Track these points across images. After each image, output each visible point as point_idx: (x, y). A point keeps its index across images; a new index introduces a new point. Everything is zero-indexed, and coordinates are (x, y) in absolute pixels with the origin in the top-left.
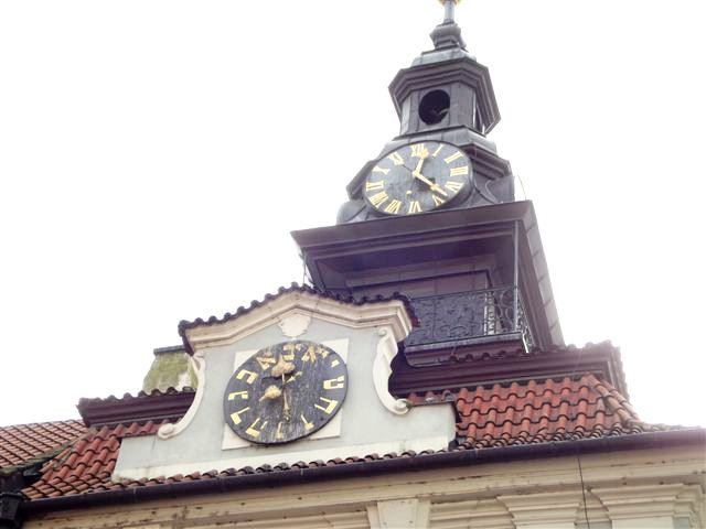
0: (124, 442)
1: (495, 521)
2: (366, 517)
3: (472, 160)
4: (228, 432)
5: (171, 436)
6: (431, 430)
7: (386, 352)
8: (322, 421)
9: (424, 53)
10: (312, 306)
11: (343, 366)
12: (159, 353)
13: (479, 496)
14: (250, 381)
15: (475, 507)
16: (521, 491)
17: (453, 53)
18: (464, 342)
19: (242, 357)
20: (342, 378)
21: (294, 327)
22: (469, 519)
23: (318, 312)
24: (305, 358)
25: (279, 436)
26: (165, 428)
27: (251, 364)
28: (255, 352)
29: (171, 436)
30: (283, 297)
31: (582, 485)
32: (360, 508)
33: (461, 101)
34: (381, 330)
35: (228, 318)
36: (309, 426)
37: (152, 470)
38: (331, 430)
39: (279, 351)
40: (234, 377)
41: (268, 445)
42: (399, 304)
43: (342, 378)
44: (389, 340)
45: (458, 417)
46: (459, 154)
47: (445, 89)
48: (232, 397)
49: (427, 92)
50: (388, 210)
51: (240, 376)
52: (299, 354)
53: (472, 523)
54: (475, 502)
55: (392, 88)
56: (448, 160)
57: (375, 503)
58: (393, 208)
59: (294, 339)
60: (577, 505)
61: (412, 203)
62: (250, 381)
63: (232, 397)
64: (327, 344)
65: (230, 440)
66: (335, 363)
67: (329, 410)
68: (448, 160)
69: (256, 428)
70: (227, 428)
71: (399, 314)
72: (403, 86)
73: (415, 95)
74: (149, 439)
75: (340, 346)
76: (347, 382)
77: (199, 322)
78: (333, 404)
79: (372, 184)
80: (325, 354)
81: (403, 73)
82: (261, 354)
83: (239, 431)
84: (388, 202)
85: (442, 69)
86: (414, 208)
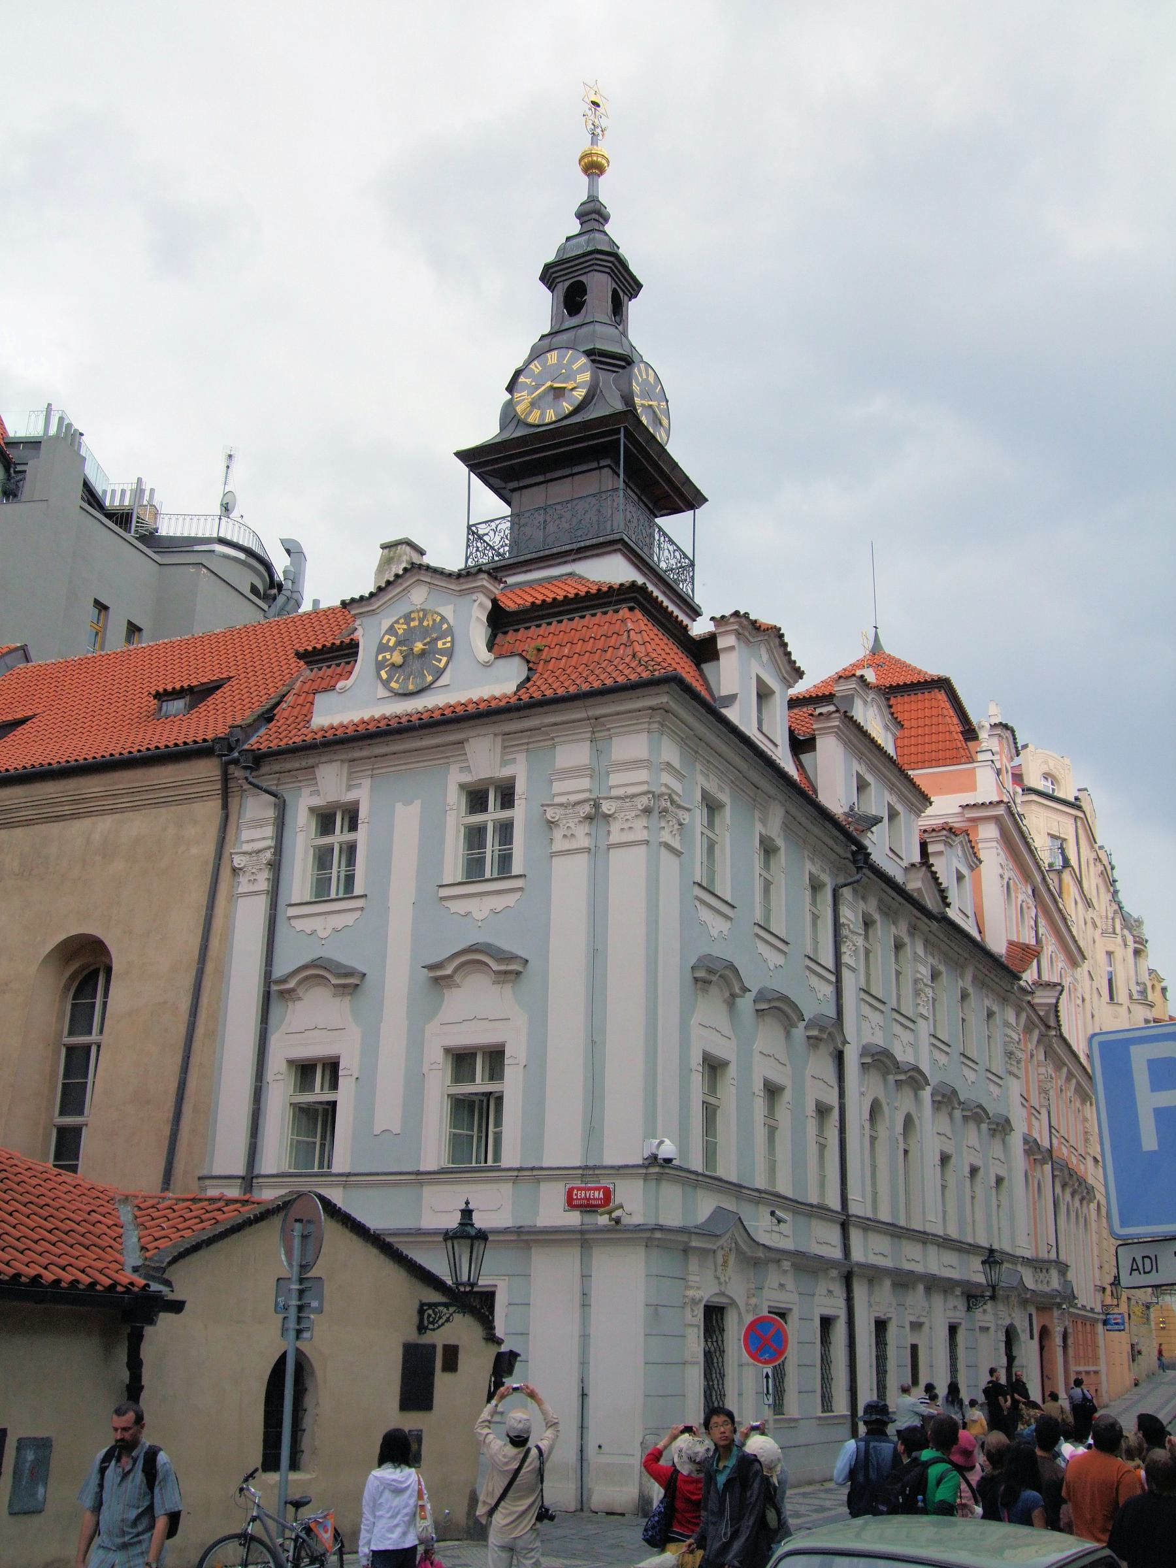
1: (542, 744)
3: (593, 361)
4: (380, 686)
5: (344, 691)
9: (568, 239)
12: (384, 547)
14: (391, 644)
15: (530, 737)
16: (555, 724)
17: (588, 242)
18: (582, 544)
19: (386, 624)
22: (528, 744)
24: (425, 623)
25: (411, 687)
26: (340, 685)
27: (391, 630)
28: (395, 619)
29: (344, 691)
30: (408, 575)
32: (461, 742)
33: (599, 285)
34: (474, 597)
35: (372, 595)
36: (430, 678)
38: (444, 680)
39: (408, 618)
40: (381, 642)
41: (405, 695)
46: (583, 360)
47: (583, 278)
48: (380, 657)
49: (567, 283)
50: (530, 420)
52: (421, 621)
53: (531, 746)
55: (542, 278)
56: (575, 367)
57: (467, 740)
58: (534, 418)
62: (391, 644)
63: (380, 657)
64: (440, 610)
65: (382, 692)
66: (445, 626)
67: (442, 665)
68: (575, 367)
71: (485, 583)
72: (549, 275)
73: (560, 285)
75: (447, 611)
77: (353, 600)
78: (444, 659)
81: (548, 267)
82: (397, 622)
83: (386, 684)
84: (531, 412)
85: (577, 262)
86: (550, 416)
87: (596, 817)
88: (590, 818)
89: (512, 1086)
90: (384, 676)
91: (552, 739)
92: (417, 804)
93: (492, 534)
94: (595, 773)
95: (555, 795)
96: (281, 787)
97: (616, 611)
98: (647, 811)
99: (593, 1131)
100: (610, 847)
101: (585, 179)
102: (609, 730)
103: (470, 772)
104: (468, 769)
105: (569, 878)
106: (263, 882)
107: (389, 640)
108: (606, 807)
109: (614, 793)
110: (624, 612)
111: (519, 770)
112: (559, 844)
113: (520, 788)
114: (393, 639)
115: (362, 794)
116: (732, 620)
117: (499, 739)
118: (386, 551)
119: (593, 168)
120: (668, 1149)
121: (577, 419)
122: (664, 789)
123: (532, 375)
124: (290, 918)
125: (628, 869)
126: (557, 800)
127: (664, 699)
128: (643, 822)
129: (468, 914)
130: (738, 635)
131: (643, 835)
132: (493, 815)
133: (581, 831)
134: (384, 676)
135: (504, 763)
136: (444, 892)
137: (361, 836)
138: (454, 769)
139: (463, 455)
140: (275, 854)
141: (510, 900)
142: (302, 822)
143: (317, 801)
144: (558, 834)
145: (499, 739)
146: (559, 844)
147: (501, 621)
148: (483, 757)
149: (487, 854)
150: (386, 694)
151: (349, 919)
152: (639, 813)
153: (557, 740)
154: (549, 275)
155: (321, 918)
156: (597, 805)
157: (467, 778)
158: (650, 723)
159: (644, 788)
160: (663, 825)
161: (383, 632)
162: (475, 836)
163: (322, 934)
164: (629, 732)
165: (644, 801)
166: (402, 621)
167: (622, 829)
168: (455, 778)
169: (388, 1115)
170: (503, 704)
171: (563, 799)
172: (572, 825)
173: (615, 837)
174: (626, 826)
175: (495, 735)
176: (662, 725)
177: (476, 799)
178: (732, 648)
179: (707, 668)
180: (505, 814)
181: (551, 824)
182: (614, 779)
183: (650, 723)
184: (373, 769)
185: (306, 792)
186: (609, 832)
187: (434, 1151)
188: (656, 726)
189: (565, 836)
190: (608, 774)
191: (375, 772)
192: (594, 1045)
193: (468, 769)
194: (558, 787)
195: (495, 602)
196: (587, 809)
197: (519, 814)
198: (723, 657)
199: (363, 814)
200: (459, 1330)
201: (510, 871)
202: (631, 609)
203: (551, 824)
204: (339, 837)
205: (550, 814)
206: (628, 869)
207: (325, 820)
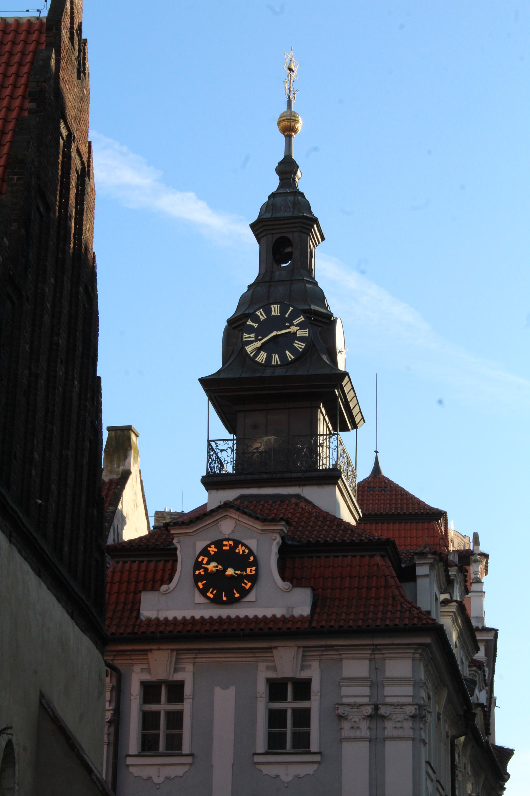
0: (142, 593)
2: (272, 652)
4: (197, 593)
5: (166, 593)
6: (299, 603)
7: (275, 549)
8: (245, 593)
10: (237, 517)
11: (255, 557)
13: (326, 646)
15: (323, 651)
19: (200, 546)
20: (254, 568)
21: (227, 527)
23: (240, 521)
26: (164, 587)
27: (205, 552)
28: (208, 543)
31: (373, 645)
32: (271, 648)
37: (160, 612)
38: (251, 597)
39: (219, 544)
42: (283, 523)
43: (254, 568)
44: (278, 542)
45: (313, 589)
47: (290, 236)
48: (197, 572)
49: (276, 237)
51: (200, 560)
54: (324, 649)
59: (227, 536)
60: (371, 652)
61: (273, 355)
62: (205, 562)
63: (197, 572)
64: (245, 541)
65: (199, 598)
69: (211, 593)
70: (196, 590)
74: (156, 593)
75: (252, 544)
76: (256, 570)
79: (248, 336)
80: (247, 551)
82: (209, 546)
83: (203, 592)
87: (376, 716)
88: (370, 717)
90: (200, 585)
91: (340, 654)
92: (232, 690)
93: (229, 451)
94: (375, 684)
95: (342, 697)
96: (115, 662)
97: (373, 556)
98: (413, 717)
100: (384, 740)
101: (282, 139)
102: (383, 654)
103: (275, 670)
104: (274, 669)
105: (355, 757)
107: (203, 559)
108: (383, 711)
109: (388, 700)
110: (378, 559)
111: (313, 672)
112: (347, 732)
113: (315, 686)
114: (206, 559)
115: (186, 675)
116: (429, 556)
117: (301, 650)
118: (113, 433)
119: (288, 129)
121: (302, 372)
122: (422, 702)
123: (256, 319)
124: (128, 766)
126: (345, 700)
127: (428, 640)
128: (408, 724)
129: (278, 776)
130: (432, 566)
131: (410, 733)
132: (289, 705)
133: (364, 725)
134: (200, 585)
135: (303, 668)
136: (257, 759)
137: (187, 707)
138: (262, 666)
139: (204, 381)
140: (113, 715)
141: (310, 769)
142: (135, 689)
143: (146, 677)
144: (346, 725)
145: (301, 650)
146: (347, 732)
147: (286, 553)
148: (286, 661)
149: (287, 732)
150: (202, 600)
151: (180, 771)
152: (407, 717)
153: (343, 656)
155: (157, 767)
156: (376, 708)
157: (272, 675)
158: (414, 653)
159: (410, 700)
160: (422, 726)
161: (198, 553)
162: (276, 718)
163: (156, 780)
164: (397, 658)
165: (411, 710)
166: (213, 546)
167: (395, 728)
168: (263, 675)
170: (306, 625)
171: (351, 700)
172: (357, 720)
173: (389, 732)
174: (398, 725)
175: (299, 647)
176: (421, 654)
177: (277, 689)
178: (427, 576)
179: (406, 587)
180: (301, 705)
181: (341, 717)
182: (388, 690)
183: (414, 653)
184: (195, 658)
185: (137, 669)
186: (384, 728)
188: (417, 656)
189: (352, 728)
190: (383, 686)
191: (196, 660)
193: (274, 669)
194: (345, 691)
195: (283, 538)
196: (369, 710)
197: (314, 705)
198: (419, 581)
199: (188, 690)
201: (308, 747)
202: (383, 556)
203: (341, 717)
204: (163, 707)
205: (341, 711)
207: (150, 691)
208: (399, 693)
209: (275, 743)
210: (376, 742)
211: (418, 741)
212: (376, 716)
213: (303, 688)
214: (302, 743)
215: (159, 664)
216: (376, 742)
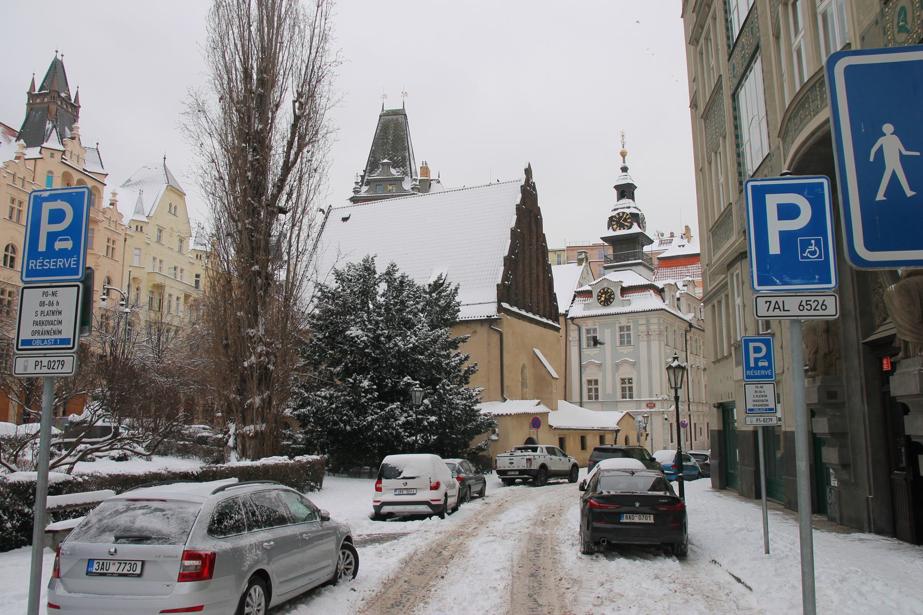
89: (634, 385)
99: (650, 395)
105: (643, 345)
106: (577, 343)
119: (623, 155)
120: (666, 397)
125: (655, 345)
132: (625, 333)
149: (625, 340)
154: (616, 187)
162: (621, 336)
169: (609, 390)
177: (621, 329)
187: (619, 398)
192: (650, 377)
197: (632, 332)
200: (643, 431)
206: (655, 345)
208: (654, 327)
209: (622, 343)
210: (649, 341)
211: (660, 341)
212: (648, 334)
213: (628, 328)
214: (629, 342)
215: (590, 324)
216: (649, 341)
